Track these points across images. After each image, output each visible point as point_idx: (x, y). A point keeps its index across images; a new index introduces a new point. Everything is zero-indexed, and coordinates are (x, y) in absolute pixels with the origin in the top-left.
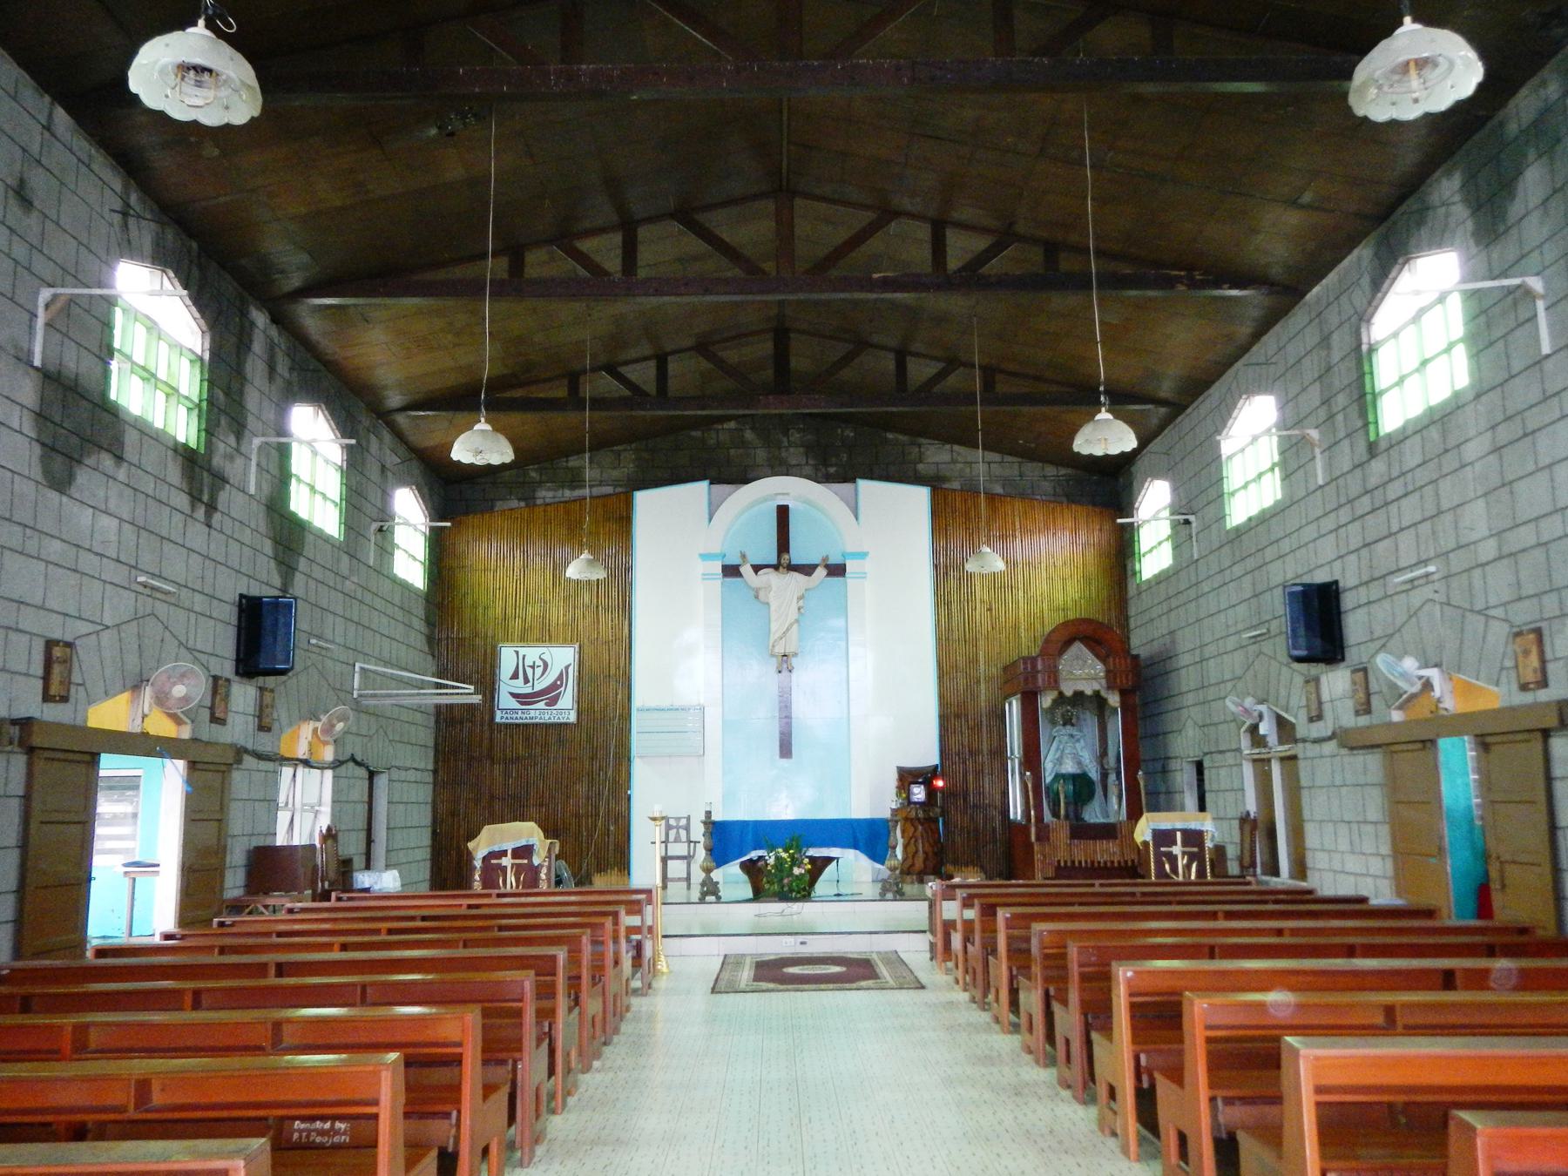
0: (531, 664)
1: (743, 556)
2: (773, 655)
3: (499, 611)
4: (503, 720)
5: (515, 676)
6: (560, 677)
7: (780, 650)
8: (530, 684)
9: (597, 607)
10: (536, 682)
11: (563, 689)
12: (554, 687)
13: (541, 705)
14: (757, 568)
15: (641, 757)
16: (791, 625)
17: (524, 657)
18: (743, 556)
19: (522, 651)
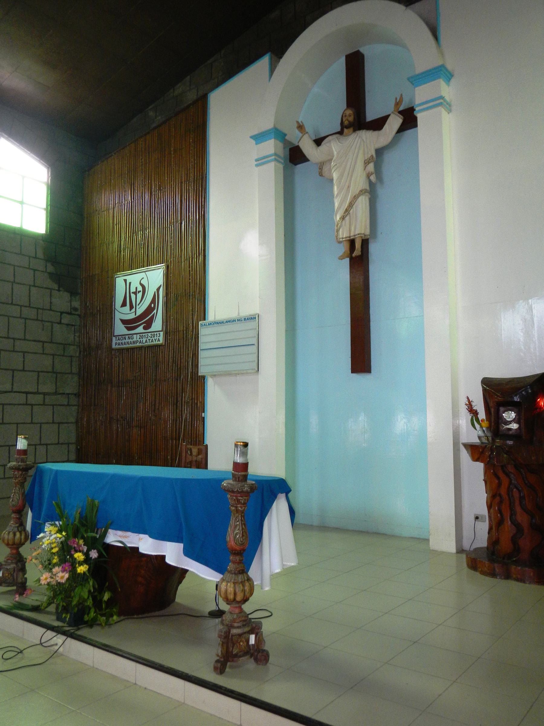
0: (135, 291)
1: (301, 127)
2: (340, 242)
3: (116, 245)
4: (117, 347)
5: (124, 304)
6: (153, 301)
7: (344, 234)
8: (134, 310)
9: (181, 223)
10: (138, 307)
11: (155, 311)
12: (149, 310)
13: (140, 329)
14: (318, 142)
15: (214, 376)
16: (355, 198)
17: (130, 283)
18: (301, 127)
19: (129, 278)
